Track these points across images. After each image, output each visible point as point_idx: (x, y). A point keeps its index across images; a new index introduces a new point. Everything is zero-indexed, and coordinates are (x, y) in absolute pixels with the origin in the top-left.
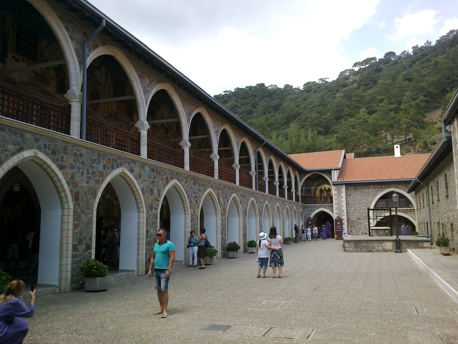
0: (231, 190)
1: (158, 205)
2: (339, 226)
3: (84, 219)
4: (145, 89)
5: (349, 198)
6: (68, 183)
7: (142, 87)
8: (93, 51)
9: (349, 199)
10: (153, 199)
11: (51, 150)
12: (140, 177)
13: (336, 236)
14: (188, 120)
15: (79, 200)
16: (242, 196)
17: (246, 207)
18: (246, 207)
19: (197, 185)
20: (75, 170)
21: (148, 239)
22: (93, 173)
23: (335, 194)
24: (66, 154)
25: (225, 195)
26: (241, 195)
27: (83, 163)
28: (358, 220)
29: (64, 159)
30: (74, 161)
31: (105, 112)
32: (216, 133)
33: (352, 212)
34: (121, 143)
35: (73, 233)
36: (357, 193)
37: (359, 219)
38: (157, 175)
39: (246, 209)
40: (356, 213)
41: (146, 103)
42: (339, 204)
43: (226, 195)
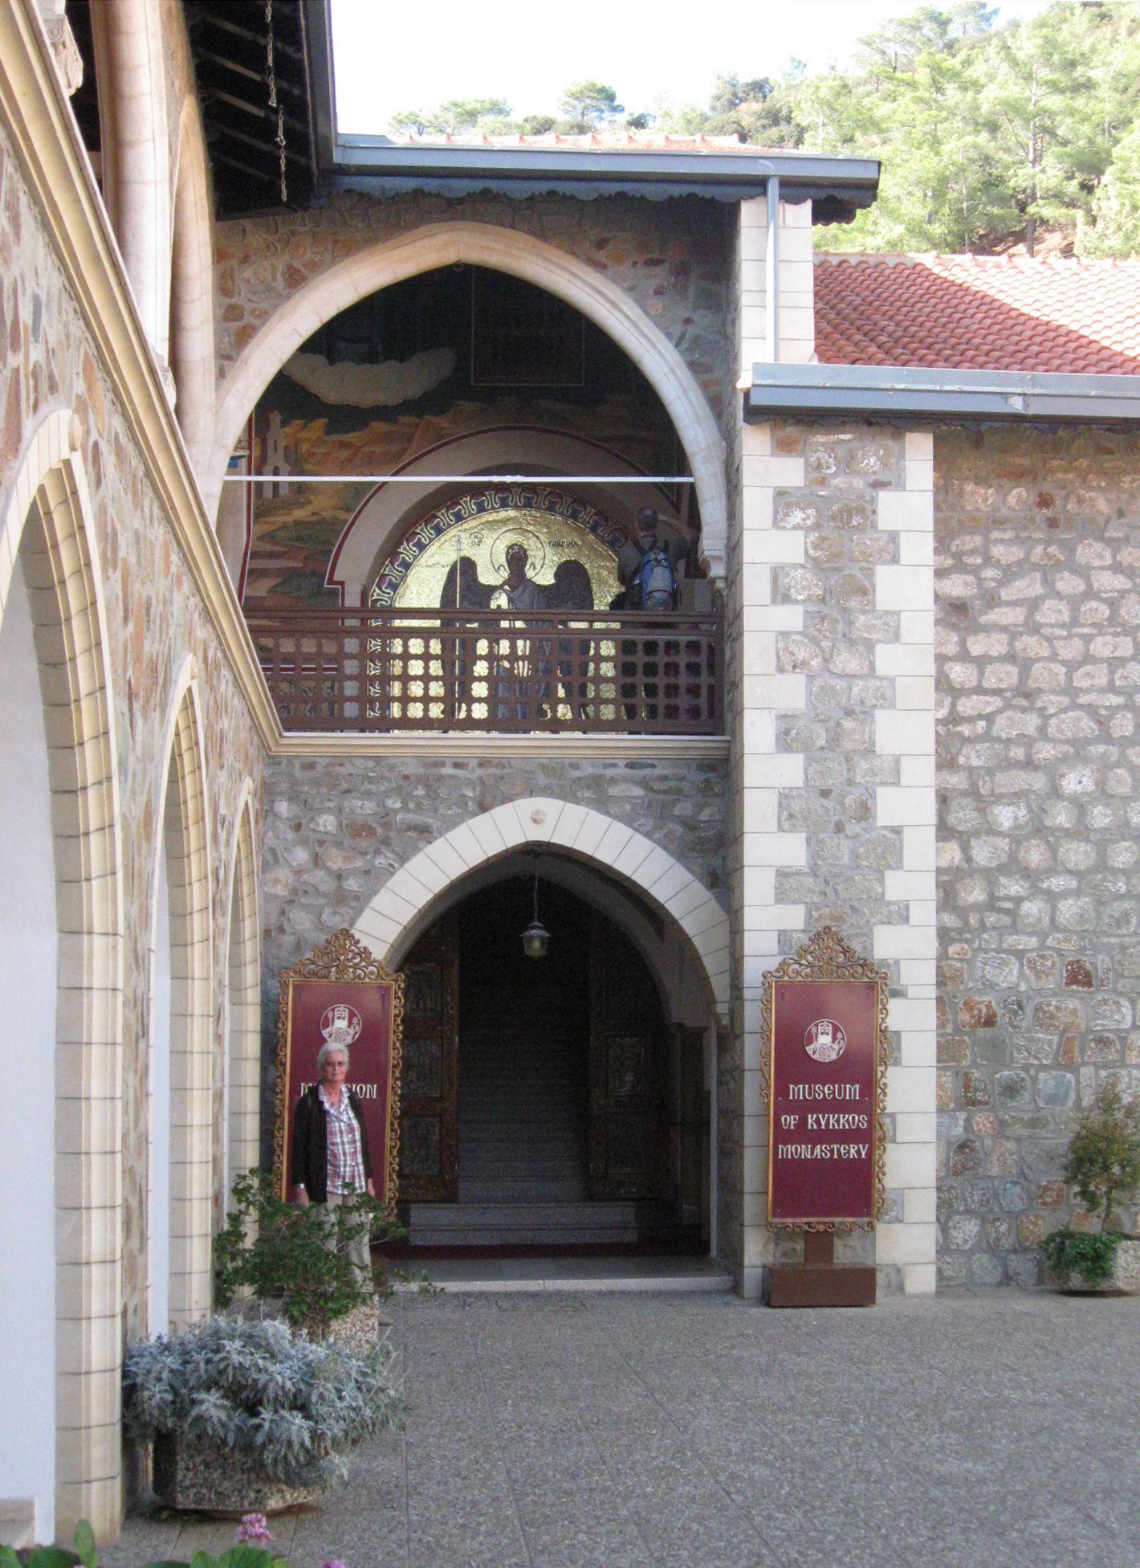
2: (824, 1091)
5: (964, 656)
9: (959, 673)
13: (756, 1252)
23: (777, 573)
28: (1073, 1003)
33: (989, 876)
36: (1068, 583)
37: (1079, 976)
40: (1057, 883)
42: (836, 738)
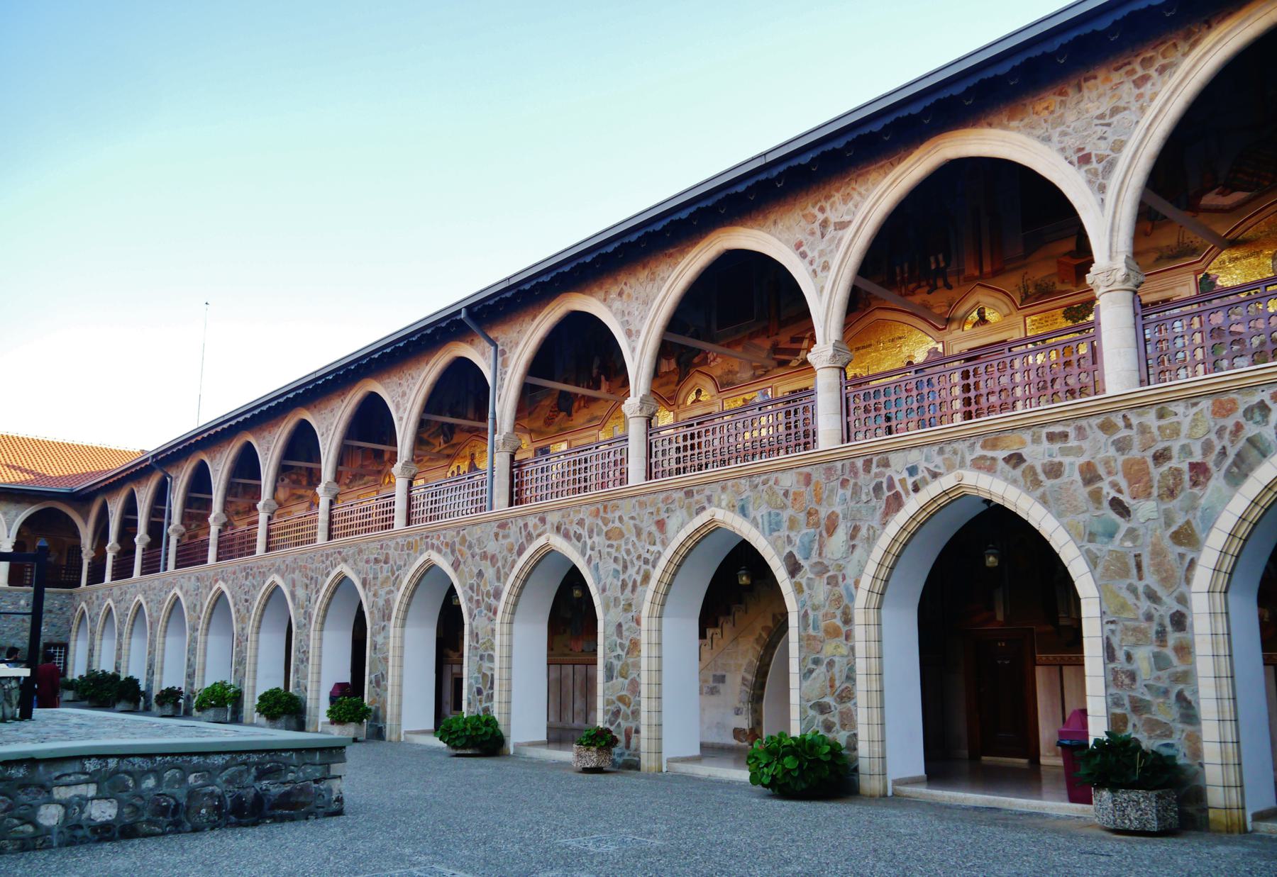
17: (390, 592)
39: (387, 602)
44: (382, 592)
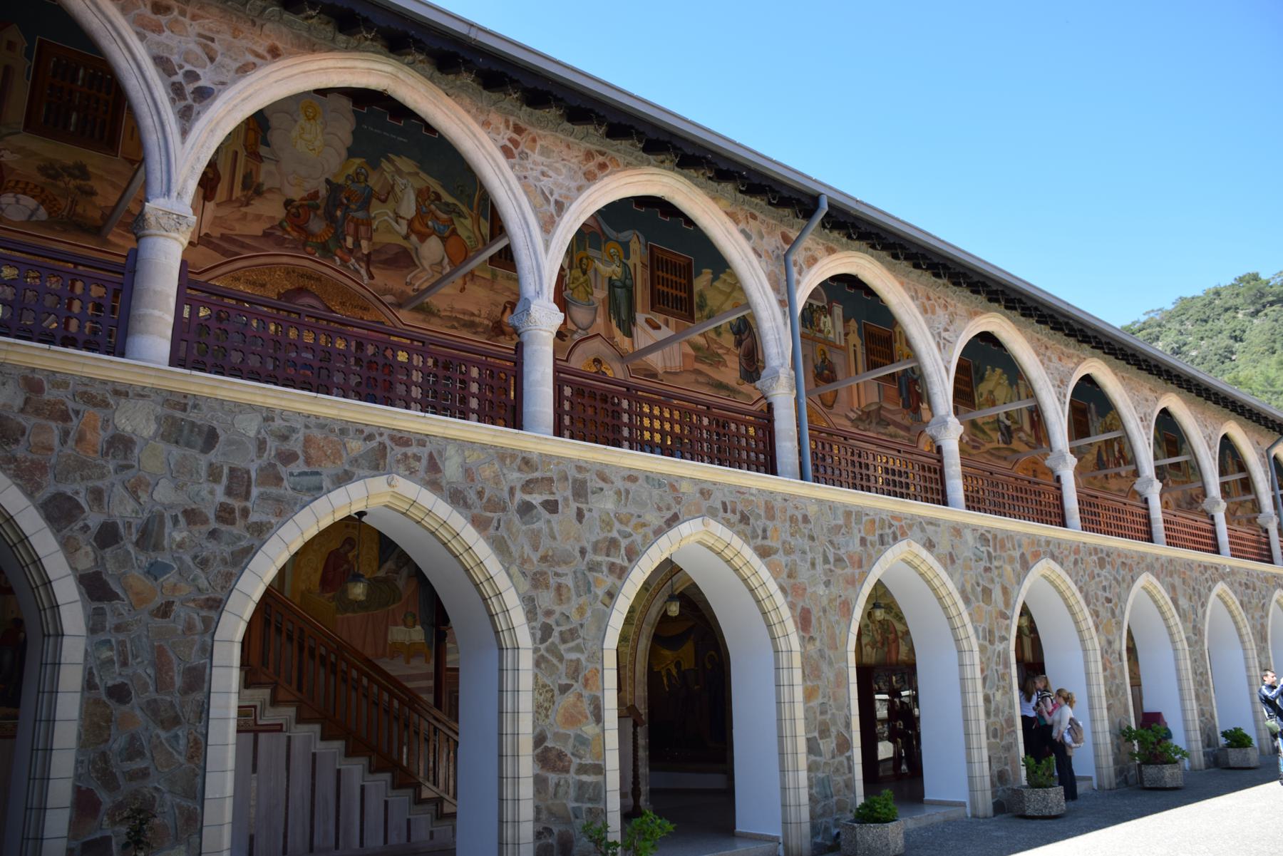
0: (1209, 572)
1: (1008, 628)
3: (828, 673)
4: (940, 337)
6: (783, 589)
7: (933, 335)
8: (808, 272)
10: (994, 615)
11: (738, 514)
12: (953, 561)
14: (1062, 399)
15: (811, 629)
16: (1244, 588)
17: (1262, 617)
18: (1262, 617)
19: (1108, 566)
20: (796, 557)
21: (992, 719)
22: (839, 560)
24: (771, 517)
25: (1194, 589)
26: (1240, 584)
27: (812, 538)
29: (769, 533)
30: (792, 535)
31: (852, 410)
32: (1142, 421)
34: (897, 478)
35: (806, 710)
38: (995, 550)
41: (947, 370)
43: (1196, 587)
44: (1257, 615)
